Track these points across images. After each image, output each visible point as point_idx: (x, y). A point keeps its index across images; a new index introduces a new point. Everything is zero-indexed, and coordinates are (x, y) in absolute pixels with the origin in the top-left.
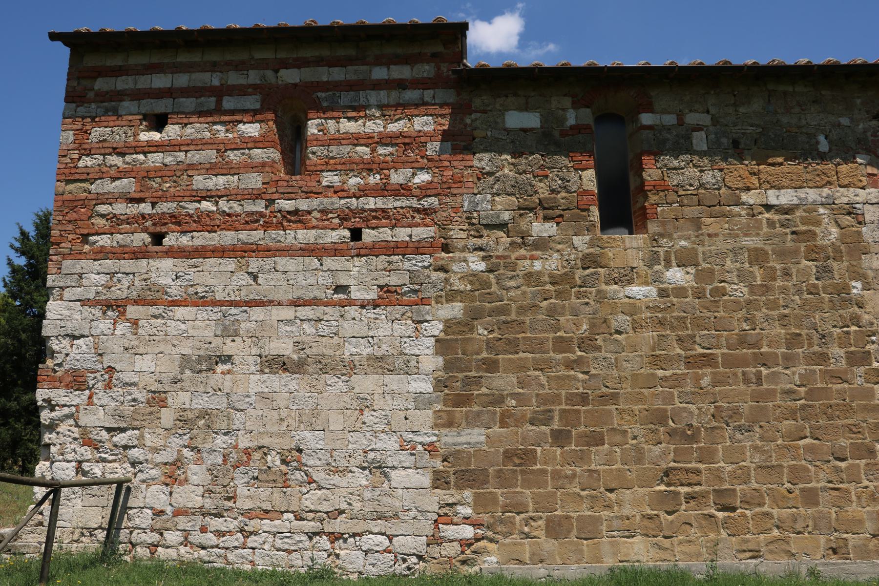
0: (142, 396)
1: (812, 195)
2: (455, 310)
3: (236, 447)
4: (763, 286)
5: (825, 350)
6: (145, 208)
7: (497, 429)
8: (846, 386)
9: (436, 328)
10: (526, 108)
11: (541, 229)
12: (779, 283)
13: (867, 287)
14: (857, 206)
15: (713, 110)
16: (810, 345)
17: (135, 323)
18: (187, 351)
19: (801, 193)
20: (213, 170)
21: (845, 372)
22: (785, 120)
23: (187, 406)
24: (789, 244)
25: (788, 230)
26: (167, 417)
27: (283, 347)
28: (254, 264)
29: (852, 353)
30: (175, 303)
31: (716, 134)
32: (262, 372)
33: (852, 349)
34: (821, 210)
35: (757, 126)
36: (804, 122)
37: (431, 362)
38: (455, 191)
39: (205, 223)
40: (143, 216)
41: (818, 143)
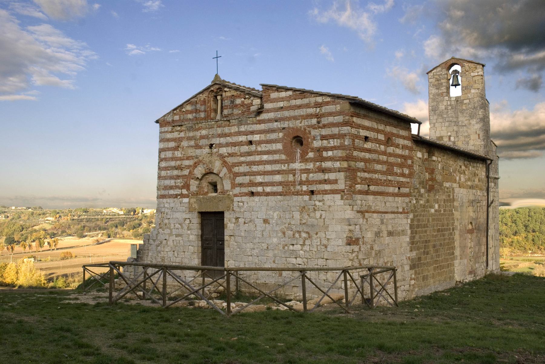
0: (369, 246)
2: (411, 216)
3: (384, 262)
6: (366, 175)
7: (417, 251)
9: (409, 221)
10: (420, 151)
11: (422, 191)
17: (367, 219)
18: (376, 230)
20: (379, 162)
23: (376, 249)
26: (373, 253)
27: (390, 228)
28: (386, 198)
30: (374, 212)
32: (388, 236)
37: (409, 232)
38: (412, 177)
39: (377, 182)
40: (366, 178)
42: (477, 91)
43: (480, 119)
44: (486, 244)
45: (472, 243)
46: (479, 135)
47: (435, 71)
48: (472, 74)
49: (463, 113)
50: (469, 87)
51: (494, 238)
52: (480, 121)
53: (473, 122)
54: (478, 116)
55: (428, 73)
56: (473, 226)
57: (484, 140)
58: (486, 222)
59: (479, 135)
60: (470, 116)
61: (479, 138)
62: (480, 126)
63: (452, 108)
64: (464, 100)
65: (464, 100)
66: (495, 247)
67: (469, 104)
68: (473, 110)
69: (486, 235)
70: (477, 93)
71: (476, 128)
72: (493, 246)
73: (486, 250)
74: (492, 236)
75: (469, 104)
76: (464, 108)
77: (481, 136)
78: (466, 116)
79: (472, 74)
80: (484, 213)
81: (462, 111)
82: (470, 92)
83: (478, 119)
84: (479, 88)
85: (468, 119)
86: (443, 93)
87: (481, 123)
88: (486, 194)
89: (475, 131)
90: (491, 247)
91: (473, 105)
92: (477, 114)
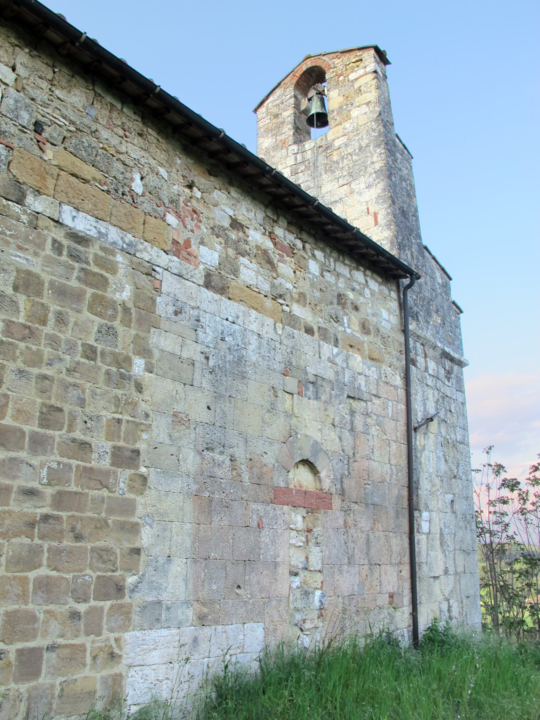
1: (114, 234)
4: (26, 327)
5: (87, 439)
8: (105, 493)
12: (49, 329)
13: (149, 369)
14: (157, 269)
15: (20, 70)
16: (71, 429)
19: (103, 227)
21: (107, 474)
22: (105, 134)
24: (74, 283)
25: (76, 265)
29: (119, 448)
31: (17, 101)
33: (121, 443)
34: (119, 258)
35: (72, 123)
36: (123, 149)
41: (132, 180)
42: (365, 109)
43: (375, 172)
44: (407, 559)
45: (315, 550)
46: (375, 215)
47: (271, 99)
48: (352, 77)
49: (333, 172)
50: (345, 107)
51: (449, 539)
52: (377, 177)
53: (360, 184)
54: (370, 170)
55: (256, 110)
56: (320, 481)
57: (388, 226)
58: (404, 480)
59: (375, 215)
60: (350, 174)
61: (376, 223)
62: (379, 191)
63: (308, 168)
64: (334, 140)
65: (334, 140)
66: (456, 573)
67: (346, 145)
68: (357, 158)
69: (406, 528)
70: (365, 113)
71: (368, 199)
72: (446, 572)
73: (407, 585)
74: (441, 534)
75: (346, 145)
76: (335, 158)
77: (380, 217)
78: (341, 177)
79: (352, 77)
80: (394, 446)
81: (329, 169)
82: (349, 117)
83: (371, 174)
84: (370, 102)
85: (345, 182)
86: (287, 138)
87: (379, 183)
88: (398, 381)
89: (364, 208)
90: (439, 571)
91: (357, 146)
92: (369, 163)
